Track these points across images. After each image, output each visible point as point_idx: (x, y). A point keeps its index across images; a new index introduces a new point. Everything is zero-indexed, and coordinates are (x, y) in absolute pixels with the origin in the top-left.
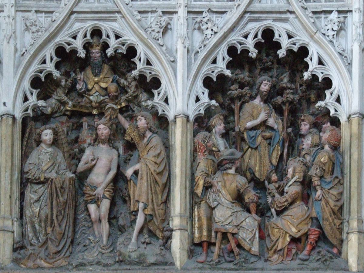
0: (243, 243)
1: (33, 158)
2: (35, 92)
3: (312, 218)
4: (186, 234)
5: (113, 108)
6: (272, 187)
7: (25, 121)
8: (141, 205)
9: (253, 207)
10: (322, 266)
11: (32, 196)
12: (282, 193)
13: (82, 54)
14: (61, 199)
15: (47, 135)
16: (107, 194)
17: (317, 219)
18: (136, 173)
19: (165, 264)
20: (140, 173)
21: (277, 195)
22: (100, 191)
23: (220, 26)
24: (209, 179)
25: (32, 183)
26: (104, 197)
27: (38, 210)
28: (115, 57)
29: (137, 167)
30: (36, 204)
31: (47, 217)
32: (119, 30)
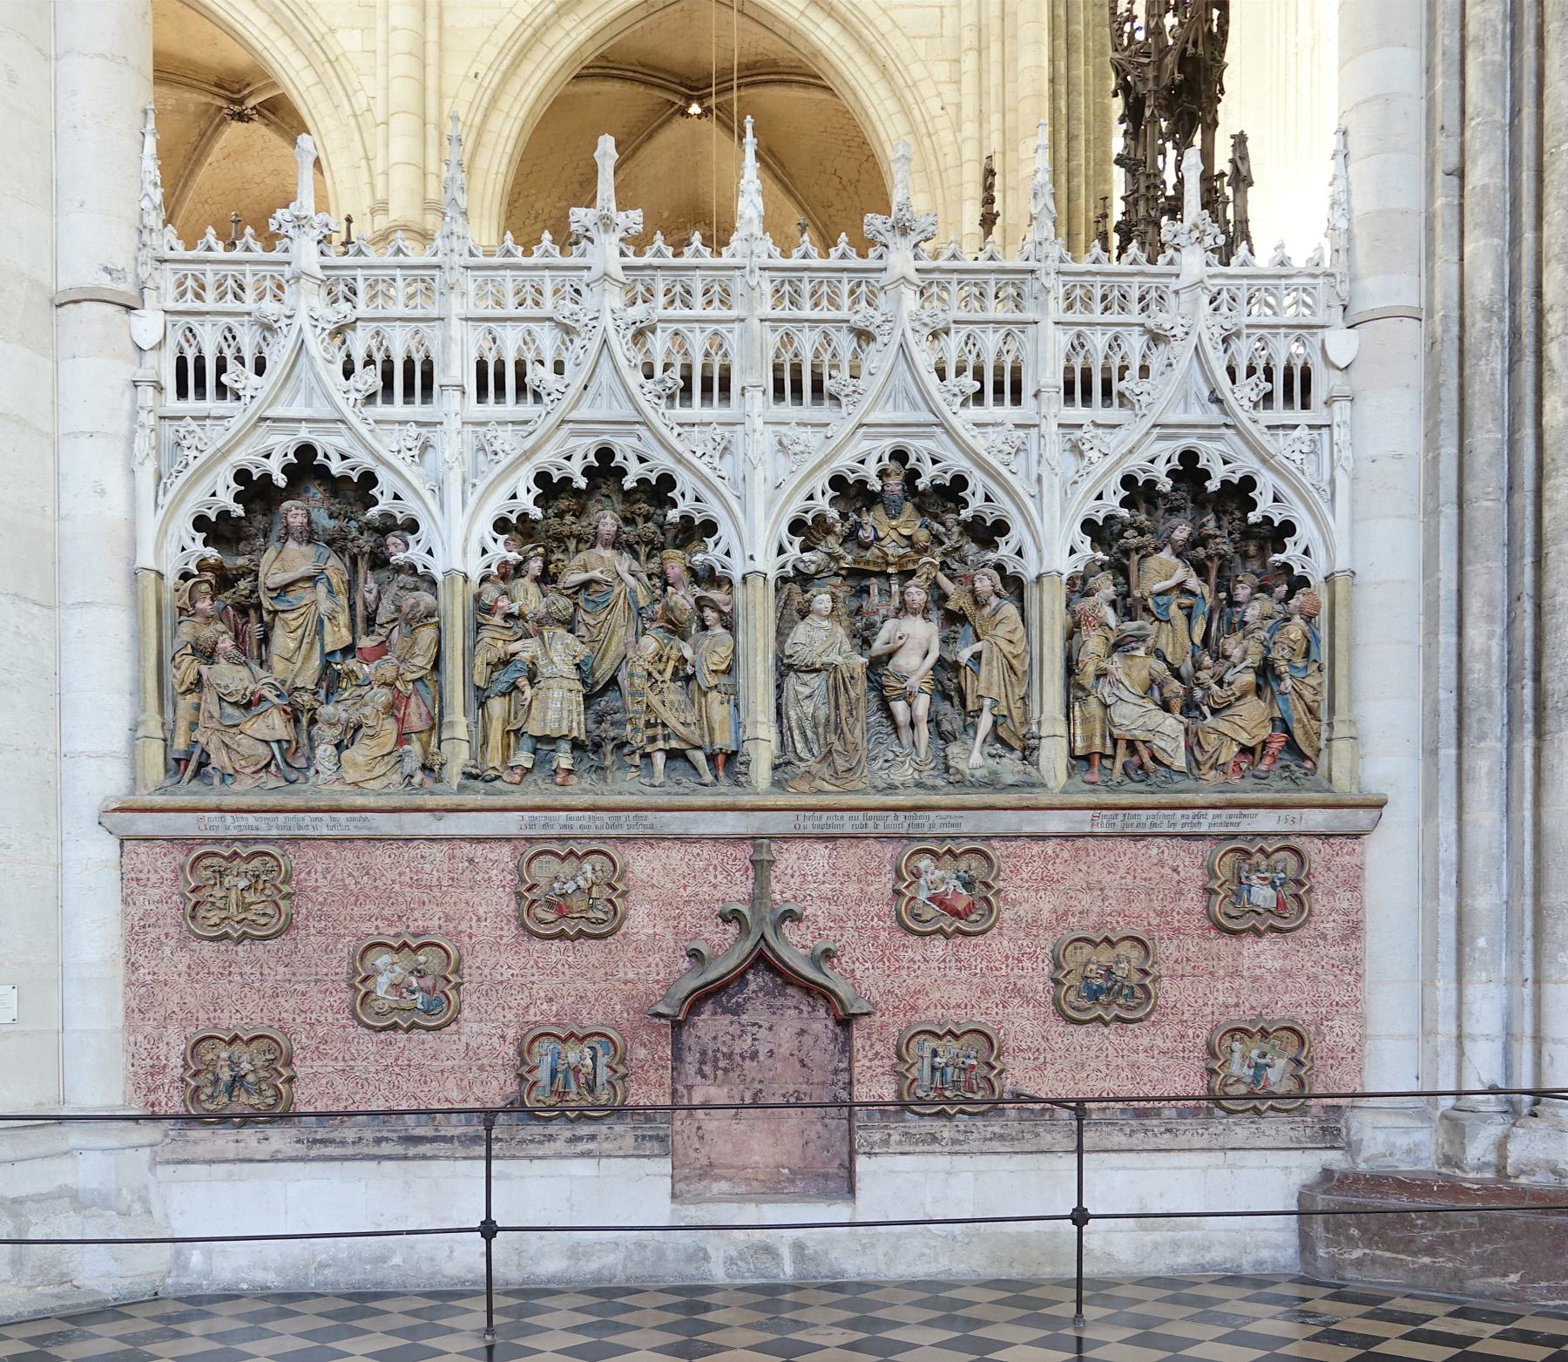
0: (1159, 755)
1: (801, 632)
2: (798, 540)
3: (1273, 720)
4: (1064, 742)
5: (931, 563)
6: (1203, 675)
7: (784, 580)
8: (987, 702)
9: (1176, 704)
10: (1292, 786)
11: (800, 689)
12: (1220, 683)
13: (875, 485)
14: (852, 694)
15: (823, 601)
16: (925, 687)
17: (1283, 720)
18: (977, 657)
19: (1033, 785)
20: (984, 656)
21: (1215, 688)
22: (914, 682)
23: (1113, 445)
24: (1103, 665)
25: (796, 671)
26: (921, 691)
27: (811, 710)
28: (938, 489)
29: (977, 647)
30: (807, 702)
31: (828, 720)
32: (938, 451)
